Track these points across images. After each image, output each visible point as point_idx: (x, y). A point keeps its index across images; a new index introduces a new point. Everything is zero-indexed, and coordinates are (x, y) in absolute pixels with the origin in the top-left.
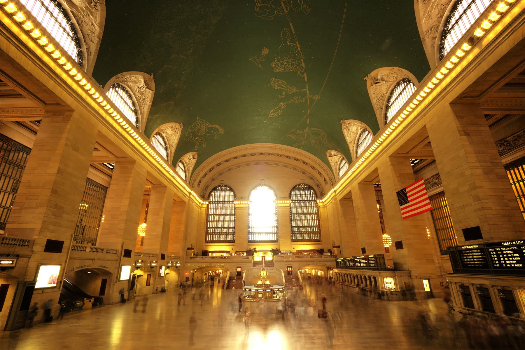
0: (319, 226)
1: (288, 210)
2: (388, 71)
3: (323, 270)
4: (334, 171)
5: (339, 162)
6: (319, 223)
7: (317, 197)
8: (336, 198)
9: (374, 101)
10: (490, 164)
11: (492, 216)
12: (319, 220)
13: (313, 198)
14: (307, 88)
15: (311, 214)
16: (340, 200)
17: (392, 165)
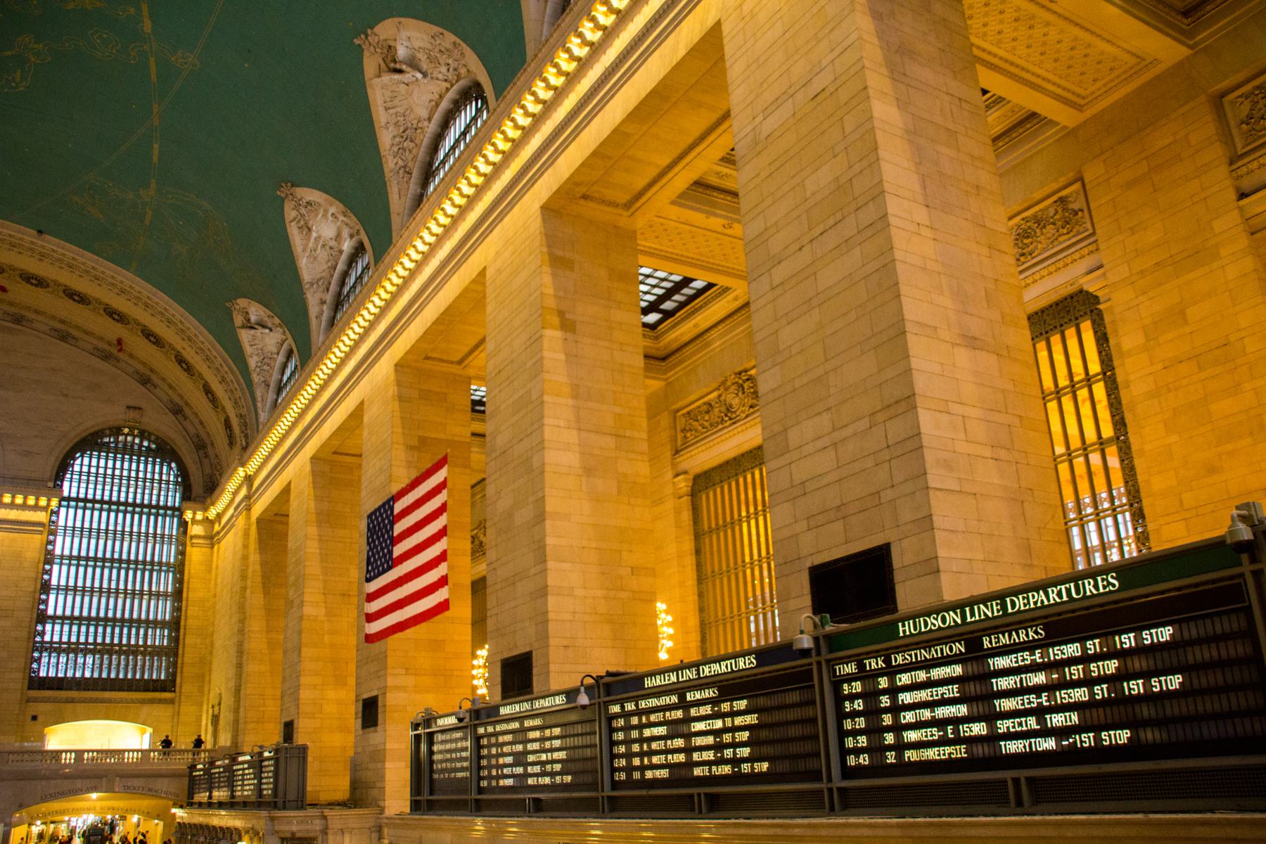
0: (175, 625)
1: (37, 540)
2: (425, 37)
3: (158, 817)
4: (258, 394)
5: (281, 359)
6: (177, 609)
7: (186, 497)
8: (249, 509)
9: (386, 139)
10: (609, 442)
11: (567, 616)
12: (178, 595)
13: (174, 499)
14: (145, 8)
15: (152, 566)
16: (259, 521)
17: (401, 398)
